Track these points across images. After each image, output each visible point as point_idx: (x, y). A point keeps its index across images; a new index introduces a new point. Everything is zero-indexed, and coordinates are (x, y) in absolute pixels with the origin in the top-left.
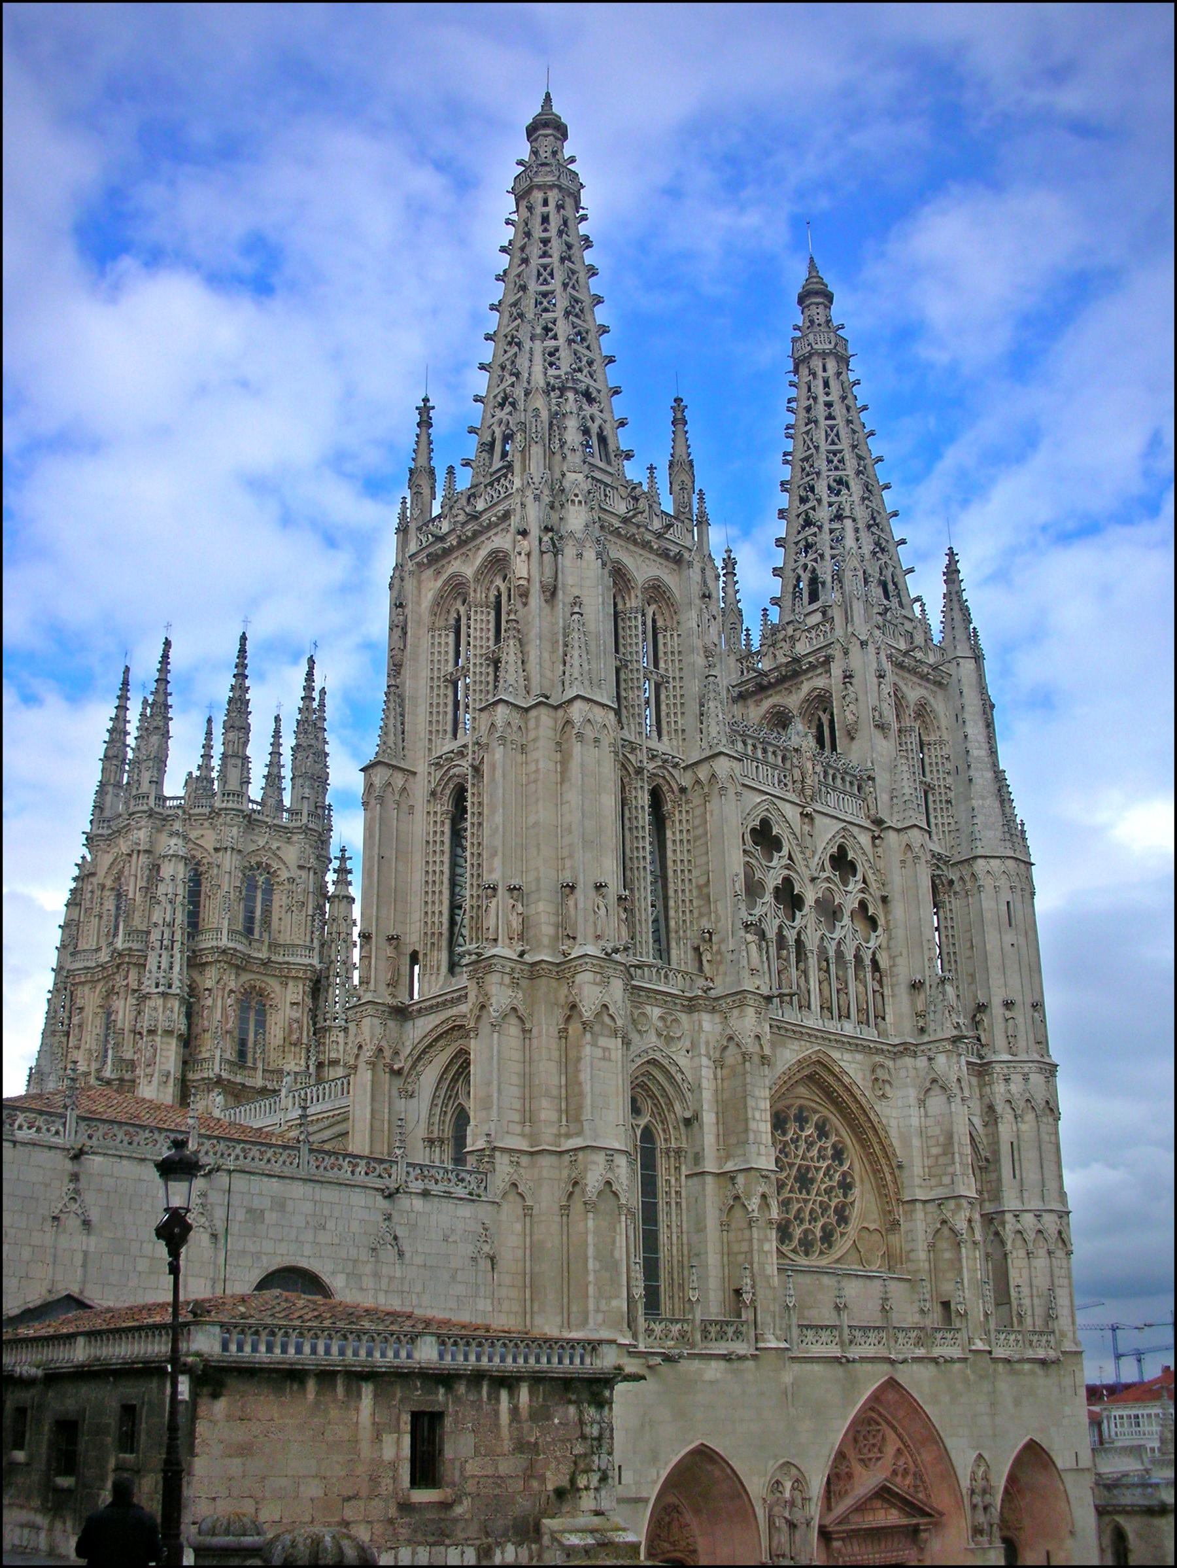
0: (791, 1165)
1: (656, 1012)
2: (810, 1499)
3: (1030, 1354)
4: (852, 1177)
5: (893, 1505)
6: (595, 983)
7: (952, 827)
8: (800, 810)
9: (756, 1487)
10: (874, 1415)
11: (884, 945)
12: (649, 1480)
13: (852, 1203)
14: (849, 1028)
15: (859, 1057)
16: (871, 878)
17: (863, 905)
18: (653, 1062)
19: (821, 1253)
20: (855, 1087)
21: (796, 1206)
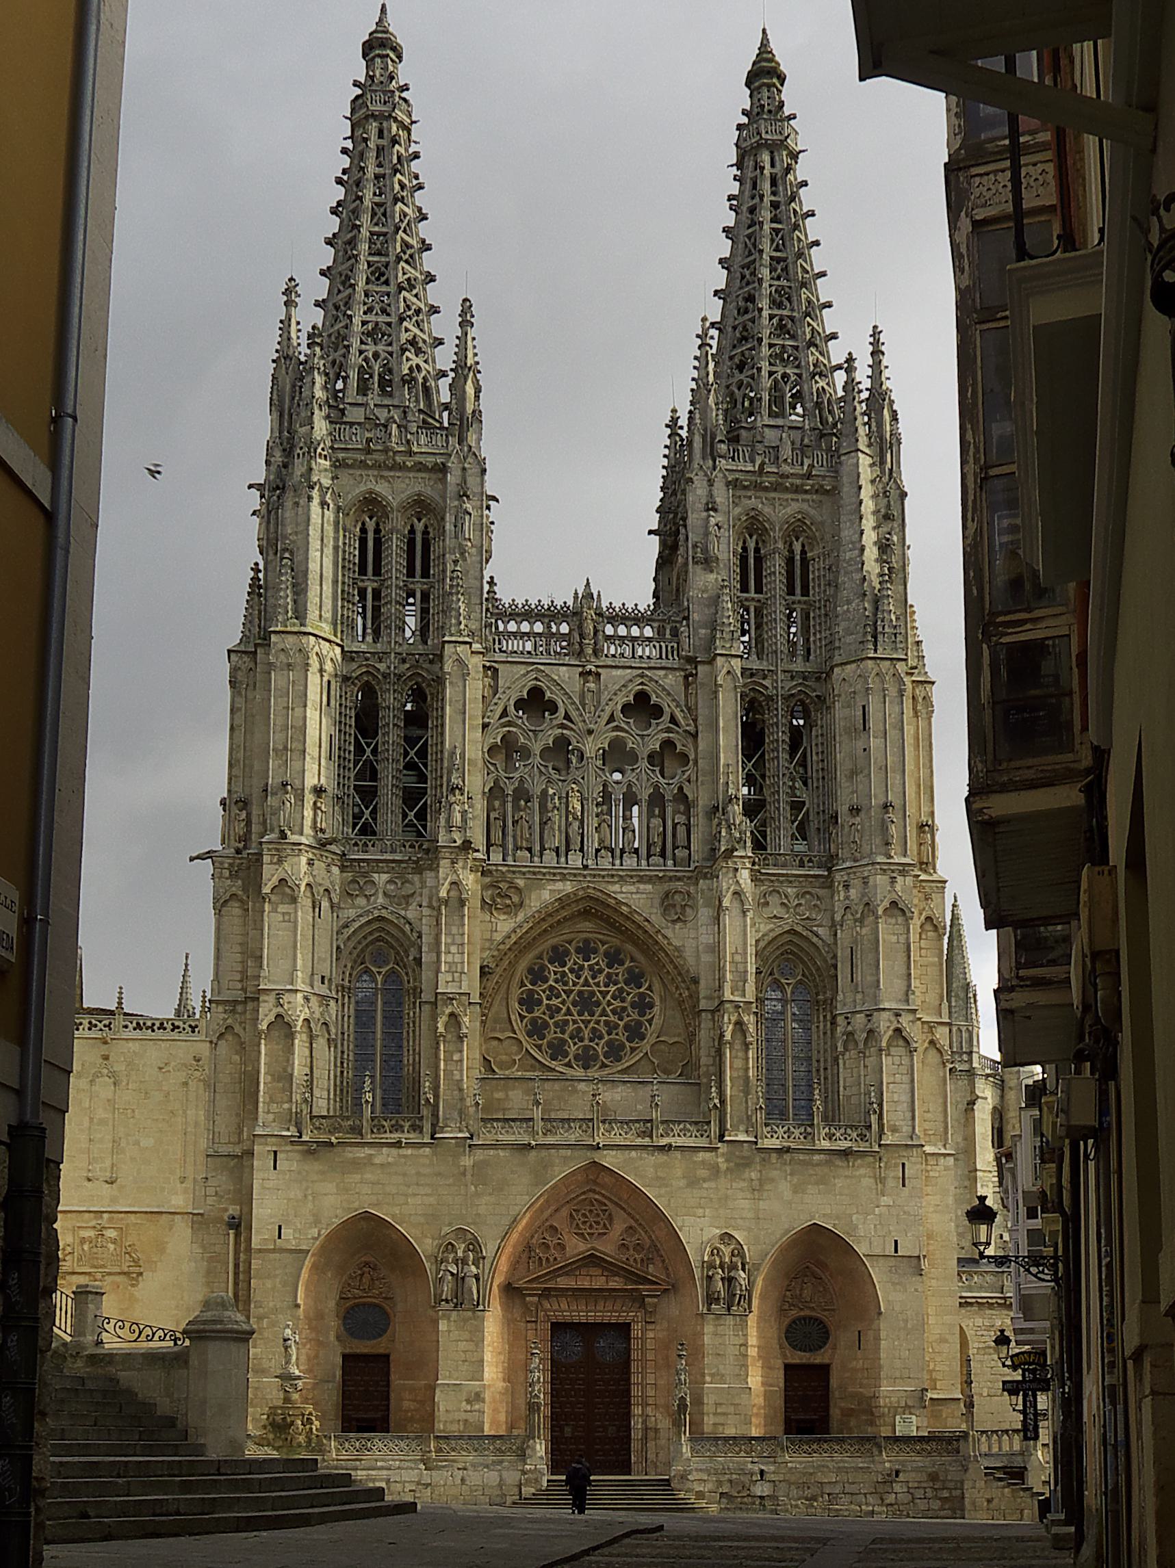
0: (568, 993)
1: (381, 878)
2: (484, 1258)
3: (826, 1144)
4: (651, 997)
5: (617, 1275)
7: (827, 641)
9: (425, 1246)
10: (597, 1197)
11: (693, 778)
12: (310, 1237)
13: (650, 1021)
14: (630, 862)
15: (649, 887)
16: (679, 716)
17: (668, 744)
18: (381, 919)
19: (604, 1066)
21: (571, 1027)
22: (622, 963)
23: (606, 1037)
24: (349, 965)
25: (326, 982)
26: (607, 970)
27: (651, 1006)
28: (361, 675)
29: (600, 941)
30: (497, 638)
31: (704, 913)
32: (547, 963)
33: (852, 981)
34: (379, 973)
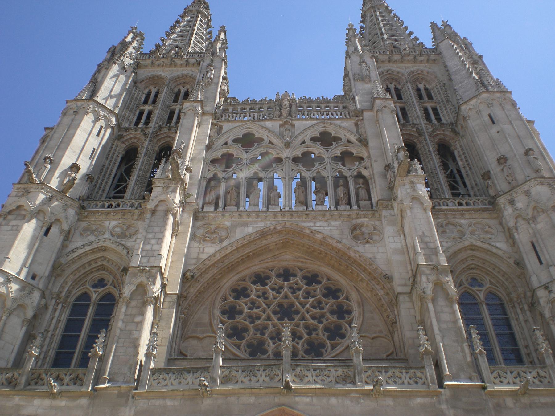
4: (348, 305)
6: (16, 196)
8: (281, 122)
16: (353, 139)
18: (104, 249)
20: (329, 240)
22: (319, 282)
23: (306, 336)
24: (70, 284)
25: (37, 279)
26: (305, 287)
27: (349, 312)
28: (131, 138)
29: (300, 269)
30: (224, 115)
31: (389, 231)
32: (249, 283)
33: (541, 263)
34: (95, 292)
